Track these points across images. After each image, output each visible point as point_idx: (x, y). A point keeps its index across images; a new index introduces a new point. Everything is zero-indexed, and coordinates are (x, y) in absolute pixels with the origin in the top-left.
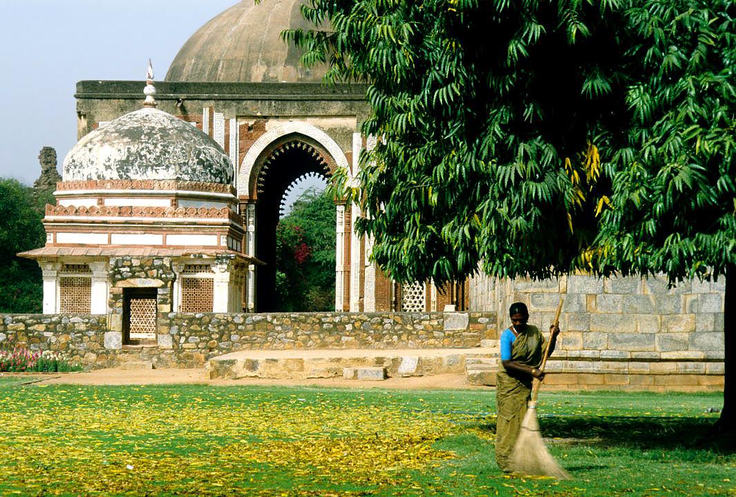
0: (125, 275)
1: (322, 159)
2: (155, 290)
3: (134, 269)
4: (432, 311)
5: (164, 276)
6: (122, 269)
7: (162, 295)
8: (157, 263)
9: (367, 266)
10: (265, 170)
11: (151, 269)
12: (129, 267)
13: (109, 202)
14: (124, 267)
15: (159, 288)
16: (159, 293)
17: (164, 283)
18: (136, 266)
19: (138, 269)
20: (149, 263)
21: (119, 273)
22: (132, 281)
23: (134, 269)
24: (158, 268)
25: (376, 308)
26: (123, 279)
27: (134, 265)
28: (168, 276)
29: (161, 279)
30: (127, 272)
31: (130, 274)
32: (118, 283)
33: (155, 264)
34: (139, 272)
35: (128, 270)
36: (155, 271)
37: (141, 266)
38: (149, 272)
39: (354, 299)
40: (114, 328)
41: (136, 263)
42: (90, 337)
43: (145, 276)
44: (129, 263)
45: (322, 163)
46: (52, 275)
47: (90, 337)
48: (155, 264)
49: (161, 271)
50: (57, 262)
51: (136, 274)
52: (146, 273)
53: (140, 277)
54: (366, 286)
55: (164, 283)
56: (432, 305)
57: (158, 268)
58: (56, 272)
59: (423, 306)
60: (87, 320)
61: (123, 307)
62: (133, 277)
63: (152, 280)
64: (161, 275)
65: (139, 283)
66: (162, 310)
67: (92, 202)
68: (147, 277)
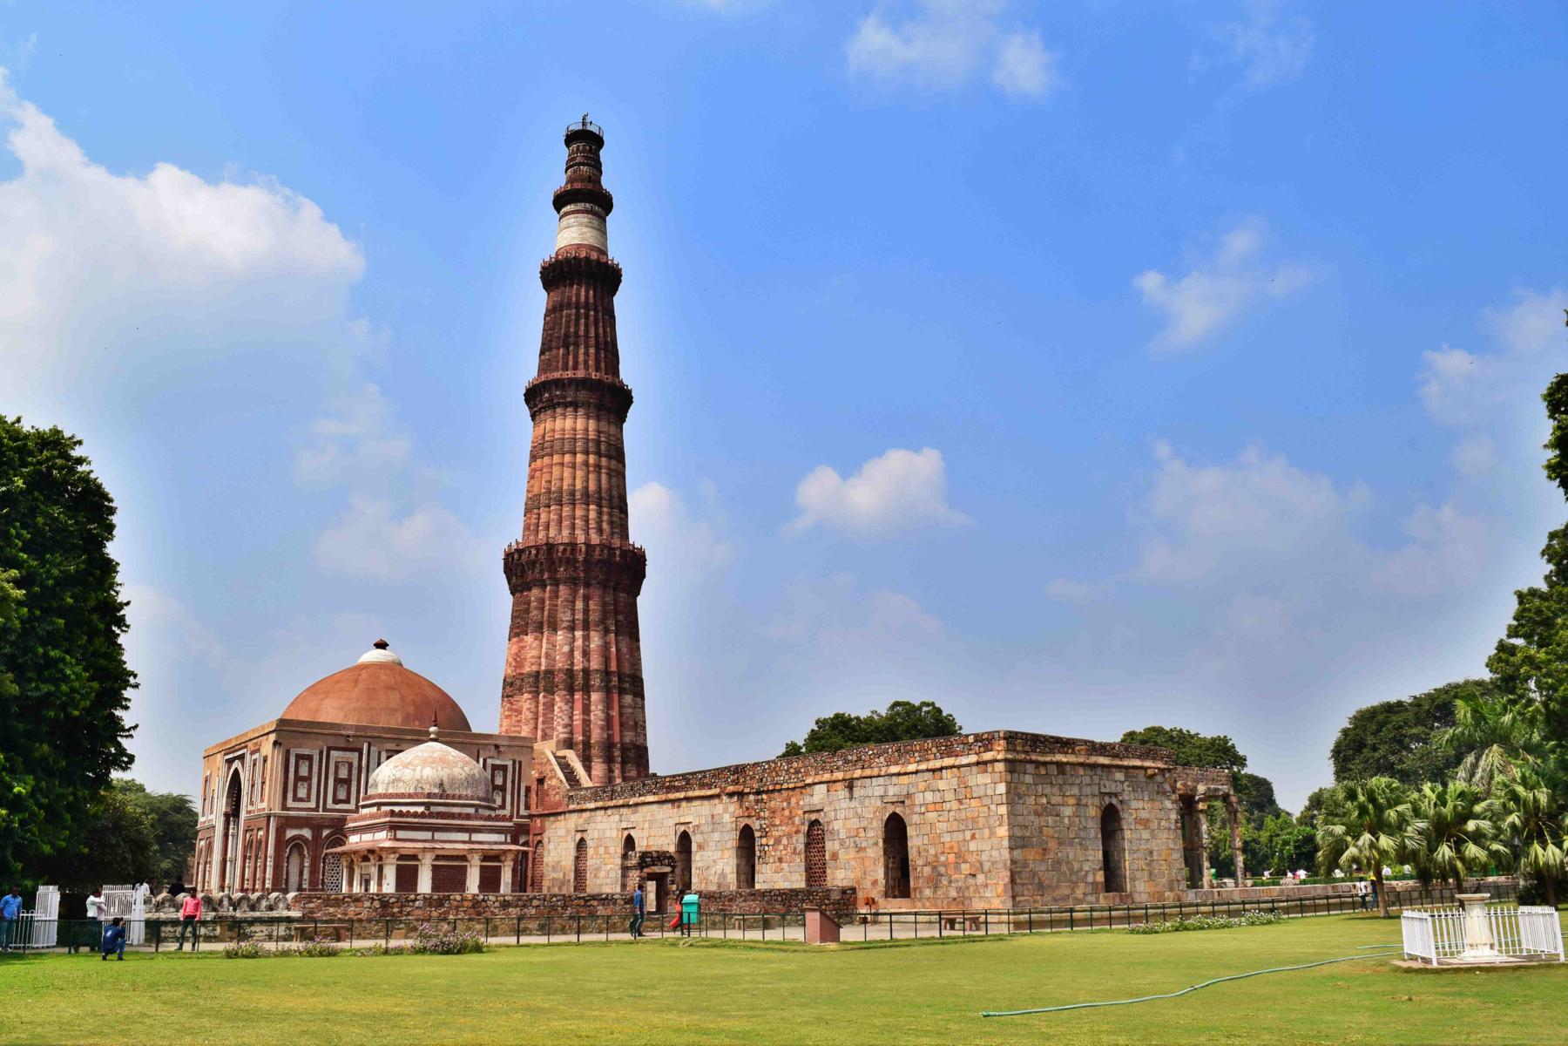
13: (433, 809)
67: (420, 809)
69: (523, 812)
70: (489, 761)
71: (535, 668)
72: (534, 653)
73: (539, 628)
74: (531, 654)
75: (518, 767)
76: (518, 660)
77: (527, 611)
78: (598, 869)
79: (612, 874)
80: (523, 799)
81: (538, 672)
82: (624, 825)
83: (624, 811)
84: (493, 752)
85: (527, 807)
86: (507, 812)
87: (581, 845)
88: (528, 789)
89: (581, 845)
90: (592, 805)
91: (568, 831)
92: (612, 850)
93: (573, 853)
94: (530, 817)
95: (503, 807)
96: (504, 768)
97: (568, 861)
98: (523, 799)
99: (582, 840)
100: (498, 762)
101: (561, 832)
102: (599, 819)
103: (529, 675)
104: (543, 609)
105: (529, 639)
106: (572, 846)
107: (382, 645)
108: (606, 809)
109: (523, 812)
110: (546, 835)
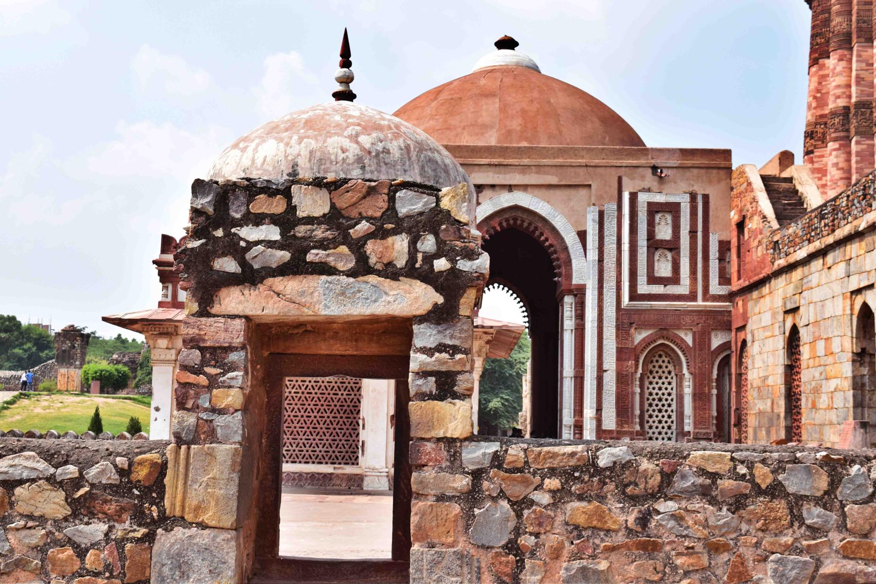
0: (258, 257)
1: (547, 239)
2: (400, 329)
3: (301, 230)
4: (687, 428)
5: (441, 264)
6: (249, 233)
7: (429, 352)
8: (410, 204)
9: (606, 371)
10: (508, 224)
11: (380, 233)
12: (275, 220)
14: (258, 220)
15: (422, 319)
16: (418, 342)
17: (440, 300)
18: (309, 220)
19: (320, 233)
20: (377, 206)
21: (237, 249)
22: (290, 285)
23: (301, 230)
24: (415, 227)
25: (617, 423)
26: (250, 277)
27: (300, 214)
28: (464, 265)
29: (428, 277)
30: (270, 244)
31: (284, 255)
32: (224, 292)
33: (403, 210)
34: (322, 244)
35: (273, 233)
36: (400, 244)
37: (335, 218)
38: (371, 247)
39: (589, 412)
40: (197, 509)
41: (311, 204)
42: (81, 553)
43: (351, 265)
44: (278, 206)
45: (547, 244)
46: (168, 357)
47: (81, 553)
48: (403, 210)
49: (428, 243)
50: (177, 334)
51: (310, 257)
52: (357, 247)
53: (330, 270)
54: (605, 396)
55: (440, 300)
56: (686, 421)
57: (415, 227)
58: (173, 352)
59: (672, 422)
60: (72, 470)
61: (245, 409)
62: (296, 267)
63: (387, 283)
64: (429, 258)
65: (321, 298)
66: (431, 426)
68: (362, 268)
69: (715, 288)
70: (643, 198)
71: (842, 103)
72: (840, 80)
73: (846, 42)
74: (834, 83)
75: (702, 205)
76: (819, 97)
77: (827, 22)
78: (817, 391)
79: (839, 402)
80: (714, 265)
81: (847, 109)
82: (855, 283)
83: (854, 249)
84: (649, 180)
85: (725, 279)
86: (683, 288)
87: (793, 341)
88: (724, 246)
89: (793, 341)
90: (802, 254)
91: (774, 315)
92: (836, 346)
93: (780, 359)
94: (731, 297)
95: (675, 279)
96: (673, 209)
97: (777, 379)
98: (714, 265)
99: (795, 330)
100: (660, 198)
101: (766, 319)
102: (814, 279)
103: (833, 114)
104: (850, 13)
105: (832, 62)
106: (780, 343)
107: (507, 43)
108: (822, 253)
109: (715, 288)
110: (749, 327)
